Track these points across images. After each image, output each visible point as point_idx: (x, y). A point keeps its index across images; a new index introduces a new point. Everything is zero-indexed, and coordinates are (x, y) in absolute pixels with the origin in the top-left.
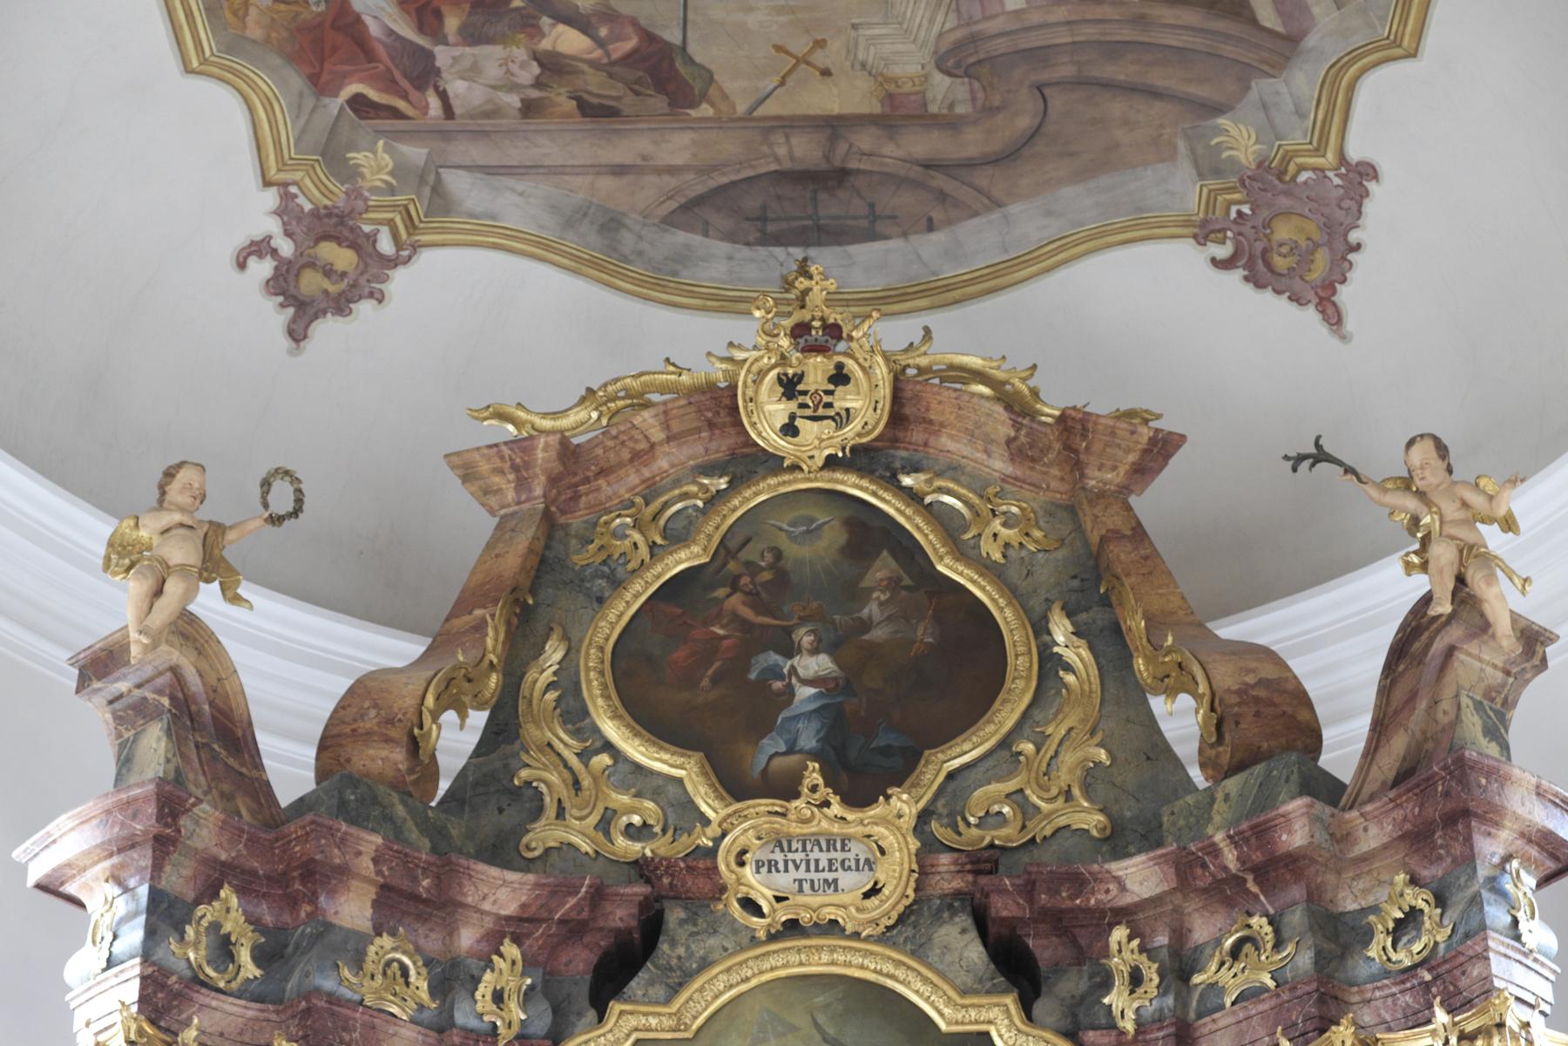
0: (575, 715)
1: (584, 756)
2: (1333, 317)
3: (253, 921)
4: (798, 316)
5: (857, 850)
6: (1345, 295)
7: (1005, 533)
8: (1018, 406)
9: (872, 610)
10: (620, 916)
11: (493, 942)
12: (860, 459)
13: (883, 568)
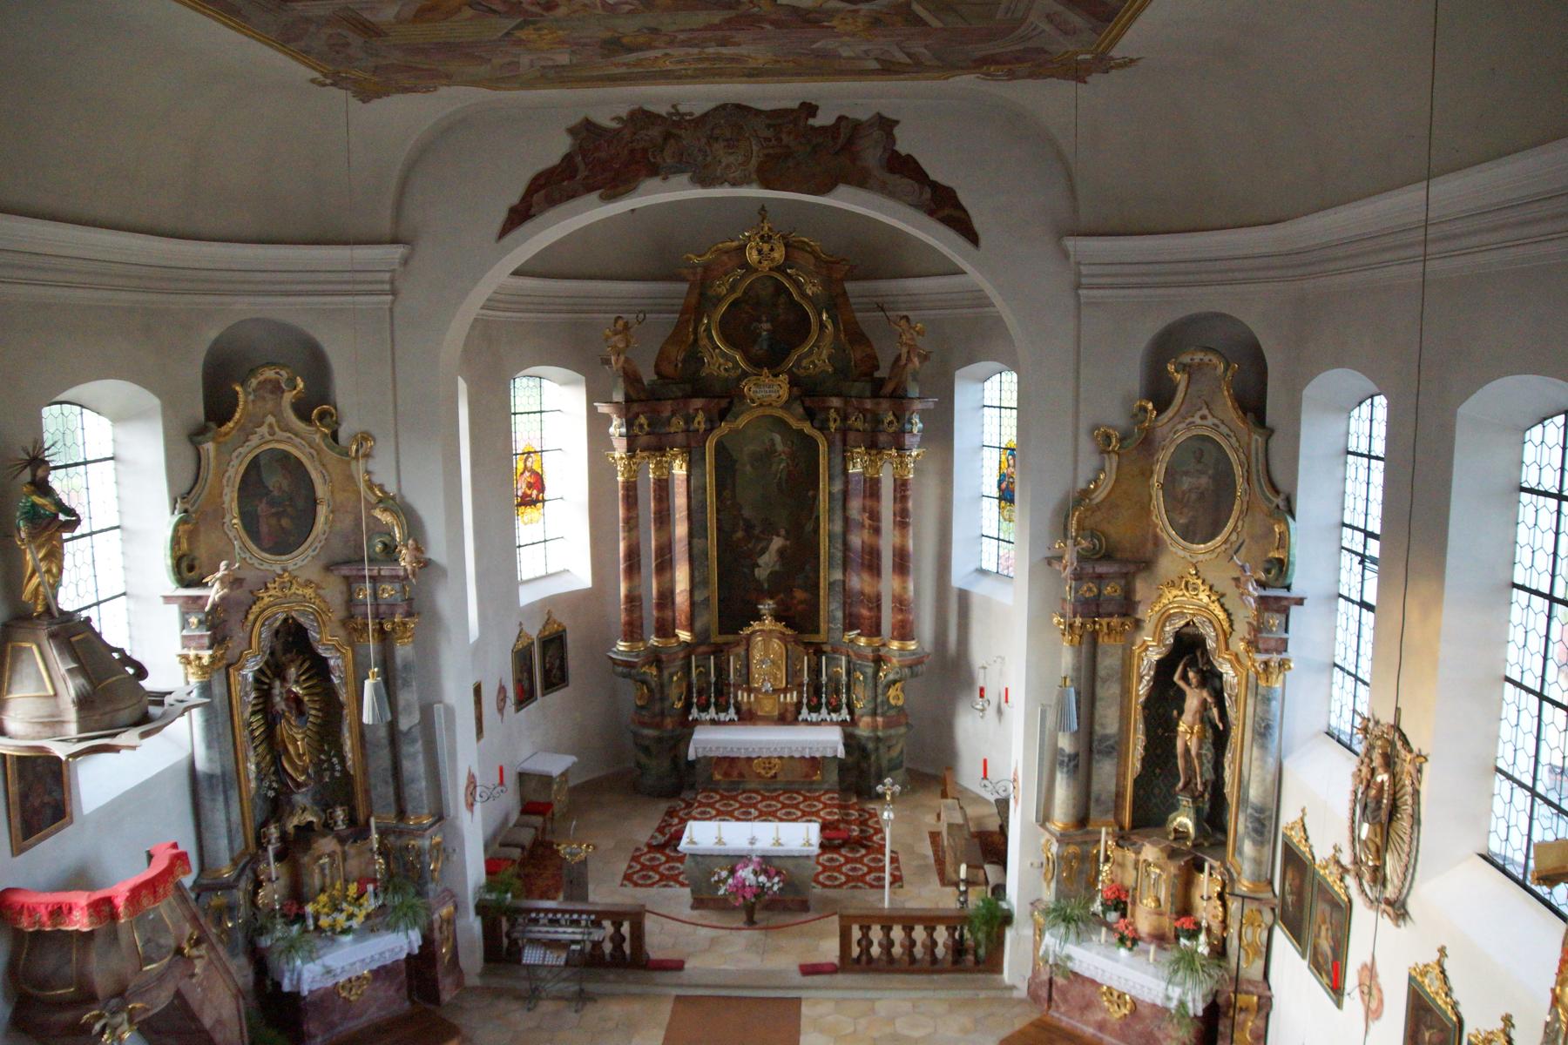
0: (711, 338)
4: (762, 233)
5: (775, 388)
7: (815, 289)
9: (781, 311)
10: (724, 403)
11: (697, 410)
12: (780, 269)
13: (782, 299)
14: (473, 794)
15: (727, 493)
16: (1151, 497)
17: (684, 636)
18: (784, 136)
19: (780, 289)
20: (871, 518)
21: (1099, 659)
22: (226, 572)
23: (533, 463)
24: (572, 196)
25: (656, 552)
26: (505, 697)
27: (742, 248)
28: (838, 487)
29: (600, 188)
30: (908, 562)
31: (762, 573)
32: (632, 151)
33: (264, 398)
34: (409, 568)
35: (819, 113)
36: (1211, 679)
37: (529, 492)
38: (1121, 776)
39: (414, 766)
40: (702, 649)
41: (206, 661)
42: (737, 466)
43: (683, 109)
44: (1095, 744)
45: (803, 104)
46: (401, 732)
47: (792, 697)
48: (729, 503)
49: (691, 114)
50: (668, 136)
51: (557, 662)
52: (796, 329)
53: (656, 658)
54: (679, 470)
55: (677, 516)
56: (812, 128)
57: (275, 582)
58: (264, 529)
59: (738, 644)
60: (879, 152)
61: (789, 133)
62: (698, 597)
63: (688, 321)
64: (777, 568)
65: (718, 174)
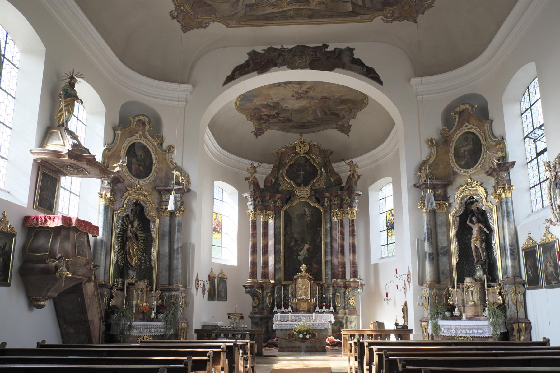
0: (283, 177)
1: (284, 181)
2: (348, 136)
3: (260, 199)
5: (306, 191)
6: (349, 134)
7: (319, 160)
8: (319, 148)
10: (288, 197)
11: (278, 199)
12: (306, 153)
13: (308, 164)
14: (198, 284)
15: (288, 229)
16: (450, 159)
17: (272, 281)
18: (317, 54)
19: (307, 160)
20: (341, 234)
21: (437, 218)
22: (122, 163)
23: (219, 216)
24: (248, 73)
25: (262, 248)
26: (205, 289)
27: (294, 148)
28: (329, 225)
29: (257, 70)
30: (355, 248)
31: (301, 258)
32: (268, 59)
33: (139, 125)
34: (185, 184)
35: (329, 47)
36: (483, 217)
37: (217, 227)
38: (451, 264)
39: (178, 262)
40: (279, 286)
41: (109, 196)
42: (292, 219)
43: (285, 47)
44: (439, 252)
45: (323, 45)
46: (174, 250)
47: (313, 300)
48: (289, 232)
49: (288, 48)
50: (280, 55)
51: (223, 290)
52: (312, 173)
53: (261, 286)
54: (271, 221)
55: (270, 238)
56: (327, 51)
57: (135, 187)
58: (133, 168)
59: (292, 283)
60: (349, 58)
61: (319, 53)
62: (277, 267)
63: (275, 170)
64: (307, 256)
65: (296, 66)
